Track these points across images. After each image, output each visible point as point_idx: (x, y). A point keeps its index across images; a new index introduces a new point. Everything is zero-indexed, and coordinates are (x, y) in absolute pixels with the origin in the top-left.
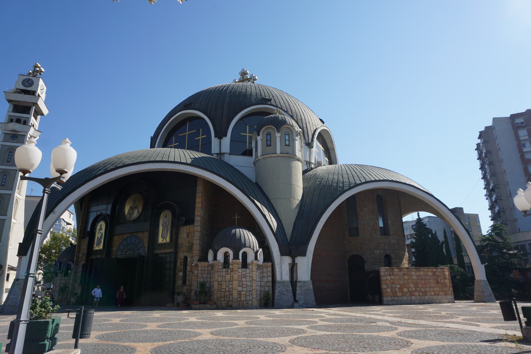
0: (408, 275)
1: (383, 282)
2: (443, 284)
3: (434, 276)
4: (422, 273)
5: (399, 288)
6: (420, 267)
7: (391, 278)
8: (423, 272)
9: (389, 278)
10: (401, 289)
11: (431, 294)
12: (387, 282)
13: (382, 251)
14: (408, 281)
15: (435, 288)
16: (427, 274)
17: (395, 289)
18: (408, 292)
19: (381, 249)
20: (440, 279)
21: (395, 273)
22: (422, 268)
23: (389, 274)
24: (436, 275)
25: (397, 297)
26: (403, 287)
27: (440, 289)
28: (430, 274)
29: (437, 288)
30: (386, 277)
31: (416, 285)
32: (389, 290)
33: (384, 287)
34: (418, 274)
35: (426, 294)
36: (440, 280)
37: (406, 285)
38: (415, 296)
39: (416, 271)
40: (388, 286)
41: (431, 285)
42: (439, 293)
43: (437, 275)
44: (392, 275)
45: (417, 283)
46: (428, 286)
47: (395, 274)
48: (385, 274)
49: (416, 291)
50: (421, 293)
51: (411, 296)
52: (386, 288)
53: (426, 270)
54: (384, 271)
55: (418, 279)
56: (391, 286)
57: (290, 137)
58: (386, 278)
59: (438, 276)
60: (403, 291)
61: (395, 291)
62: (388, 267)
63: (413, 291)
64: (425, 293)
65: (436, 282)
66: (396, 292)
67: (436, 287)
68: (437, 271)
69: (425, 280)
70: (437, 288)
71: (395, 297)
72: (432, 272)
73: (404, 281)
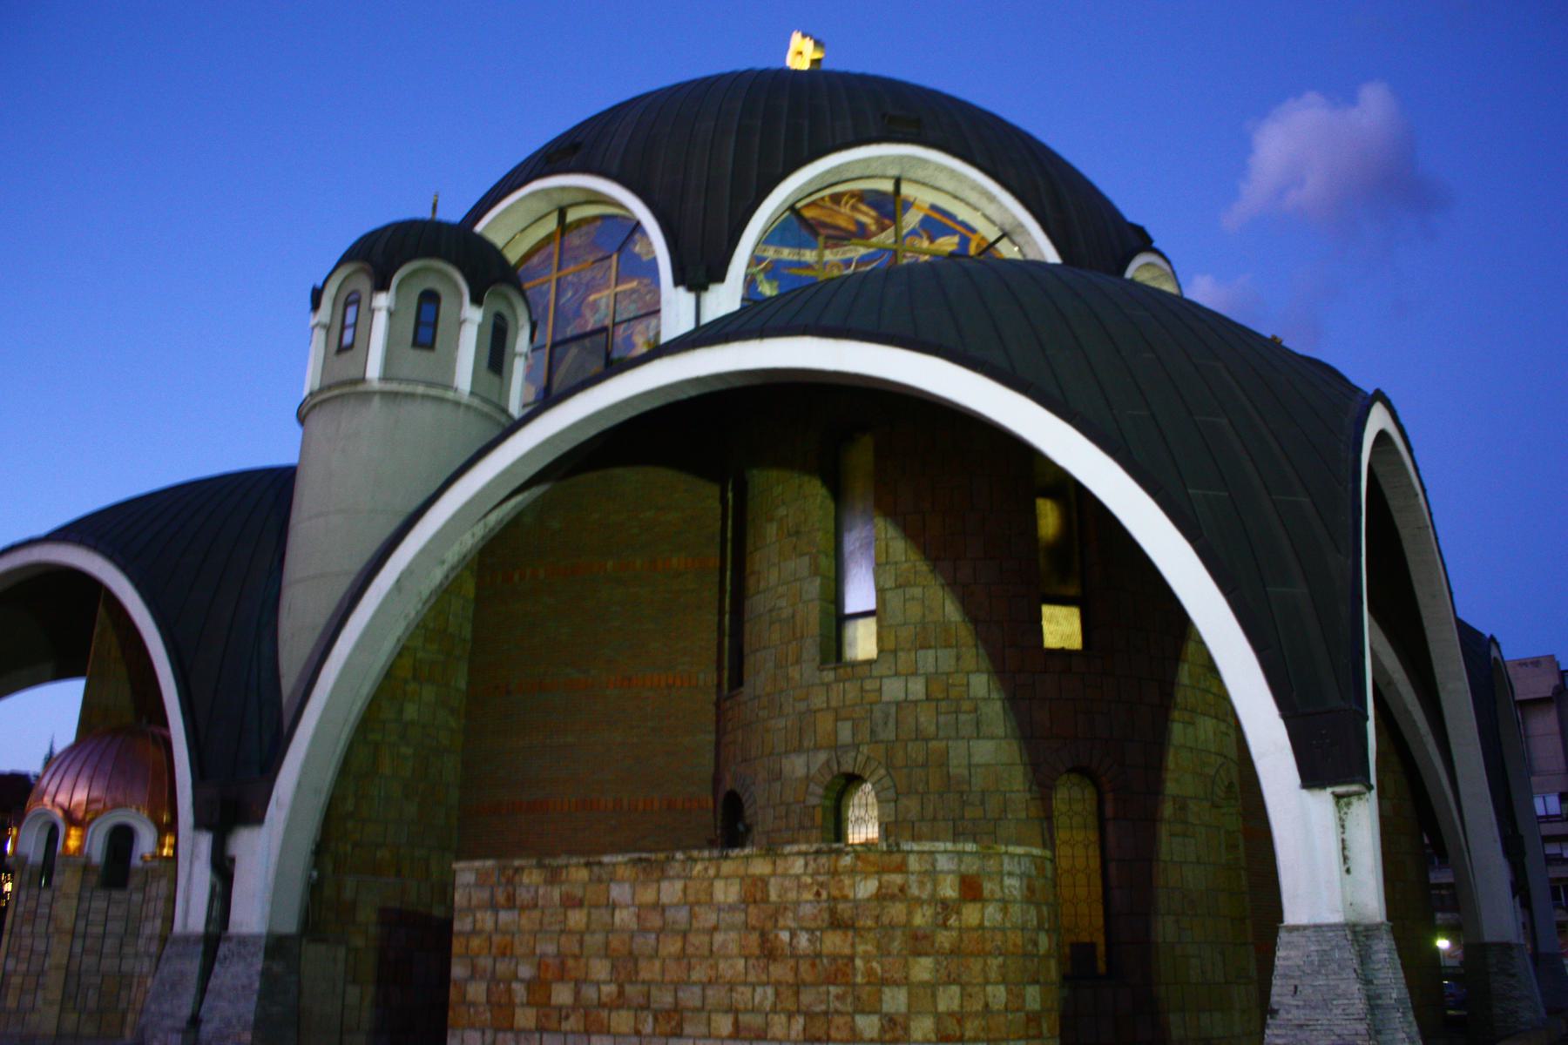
0: (591, 906)
1: (457, 946)
2: (804, 967)
3: (752, 909)
4: (671, 891)
5: (530, 985)
6: (661, 856)
7: (496, 922)
8: (679, 885)
9: (486, 920)
10: (539, 988)
11: (709, 1024)
12: (476, 943)
13: (822, 757)
14: (581, 943)
15: (741, 989)
16: (703, 897)
17: (509, 991)
18: (574, 1008)
19: (817, 748)
20: (783, 929)
21: (524, 896)
22: (679, 856)
23: (492, 895)
24: (766, 900)
25: (510, 1036)
26: (549, 976)
27: (777, 994)
28: (728, 892)
29: (759, 990)
30: (469, 920)
31: (626, 963)
32: (477, 991)
33: (458, 971)
34: (648, 895)
35: (680, 1025)
36: (785, 936)
37: (571, 963)
38: (608, 1033)
39: (641, 877)
40: (474, 968)
41: (715, 967)
42: (767, 1024)
43: (773, 897)
44: (503, 908)
45: (633, 957)
46: (695, 976)
47: (518, 903)
48: (470, 900)
49: (620, 1001)
50: (650, 1019)
51: (588, 1032)
52: (466, 981)
53: (706, 869)
54: (468, 885)
55: (643, 930)
56: (489, 969)
57: (361, 310)
58: (475, 921)
59: (779, 910)
60: (549, 997)
61: (504, 1000)
62: (489, 863)
63: (601, 1005)
64: (673, 1023)
65: (757, 951)
66: (511, 1004)
67: (754, 986)
68: (779, 870)
69: (684, 935)
70: (759, 990)
71: (500, 1036)
72: (742, 879)
73: (563, 939)
